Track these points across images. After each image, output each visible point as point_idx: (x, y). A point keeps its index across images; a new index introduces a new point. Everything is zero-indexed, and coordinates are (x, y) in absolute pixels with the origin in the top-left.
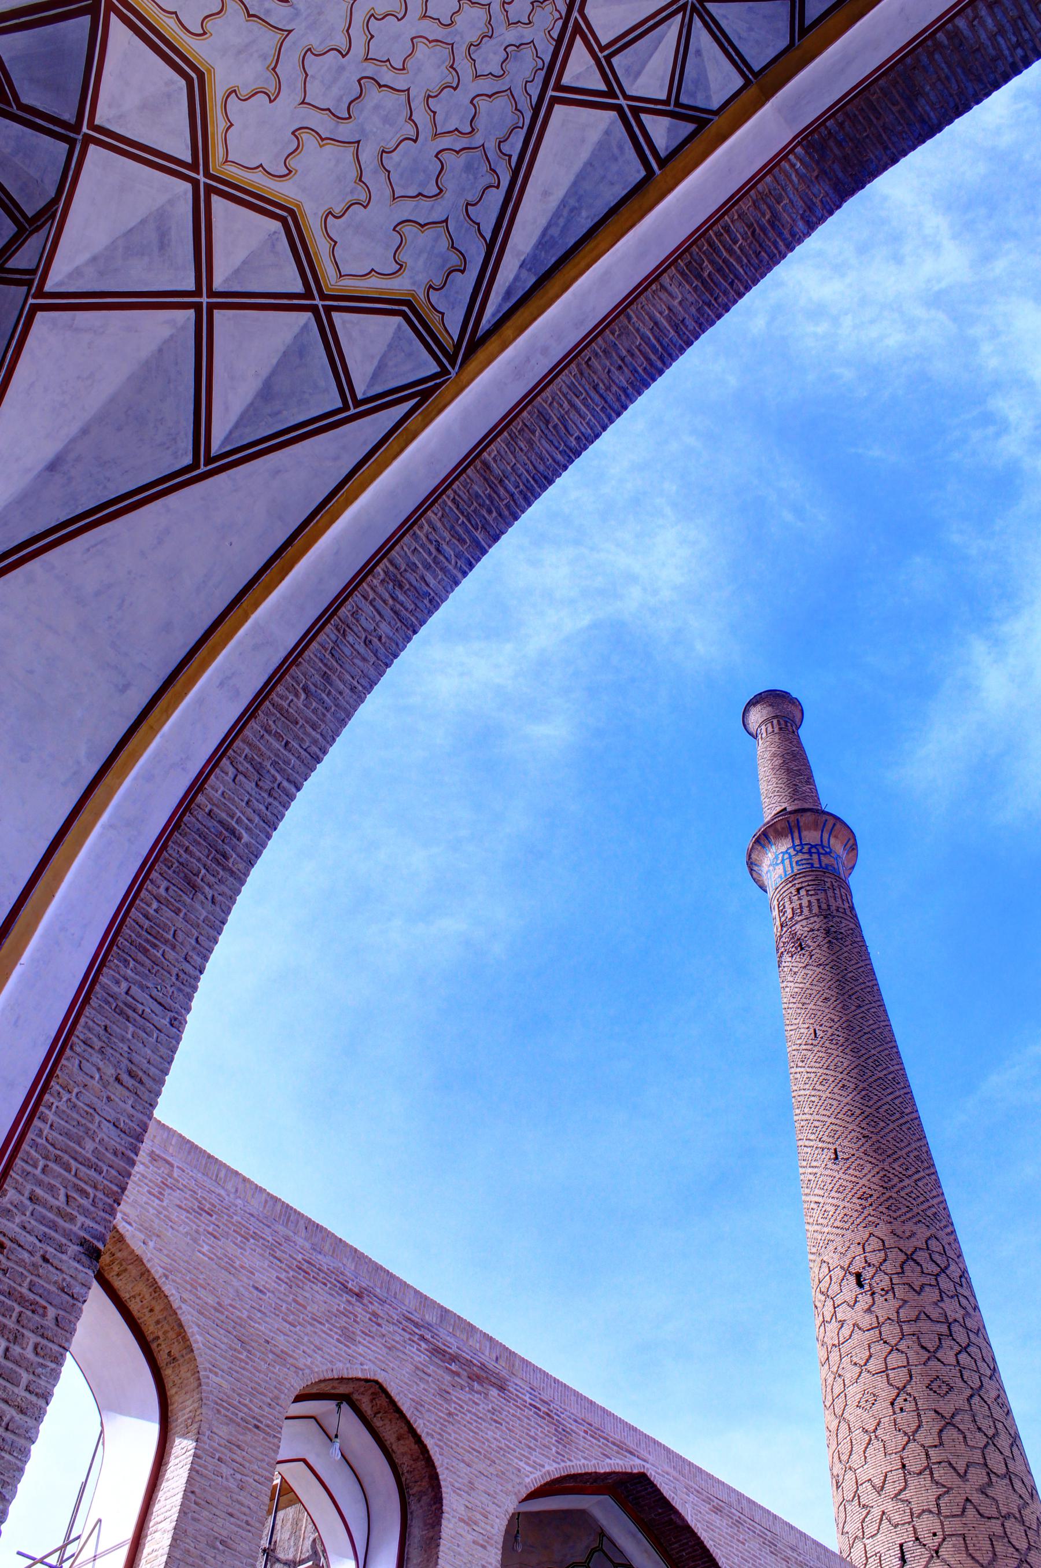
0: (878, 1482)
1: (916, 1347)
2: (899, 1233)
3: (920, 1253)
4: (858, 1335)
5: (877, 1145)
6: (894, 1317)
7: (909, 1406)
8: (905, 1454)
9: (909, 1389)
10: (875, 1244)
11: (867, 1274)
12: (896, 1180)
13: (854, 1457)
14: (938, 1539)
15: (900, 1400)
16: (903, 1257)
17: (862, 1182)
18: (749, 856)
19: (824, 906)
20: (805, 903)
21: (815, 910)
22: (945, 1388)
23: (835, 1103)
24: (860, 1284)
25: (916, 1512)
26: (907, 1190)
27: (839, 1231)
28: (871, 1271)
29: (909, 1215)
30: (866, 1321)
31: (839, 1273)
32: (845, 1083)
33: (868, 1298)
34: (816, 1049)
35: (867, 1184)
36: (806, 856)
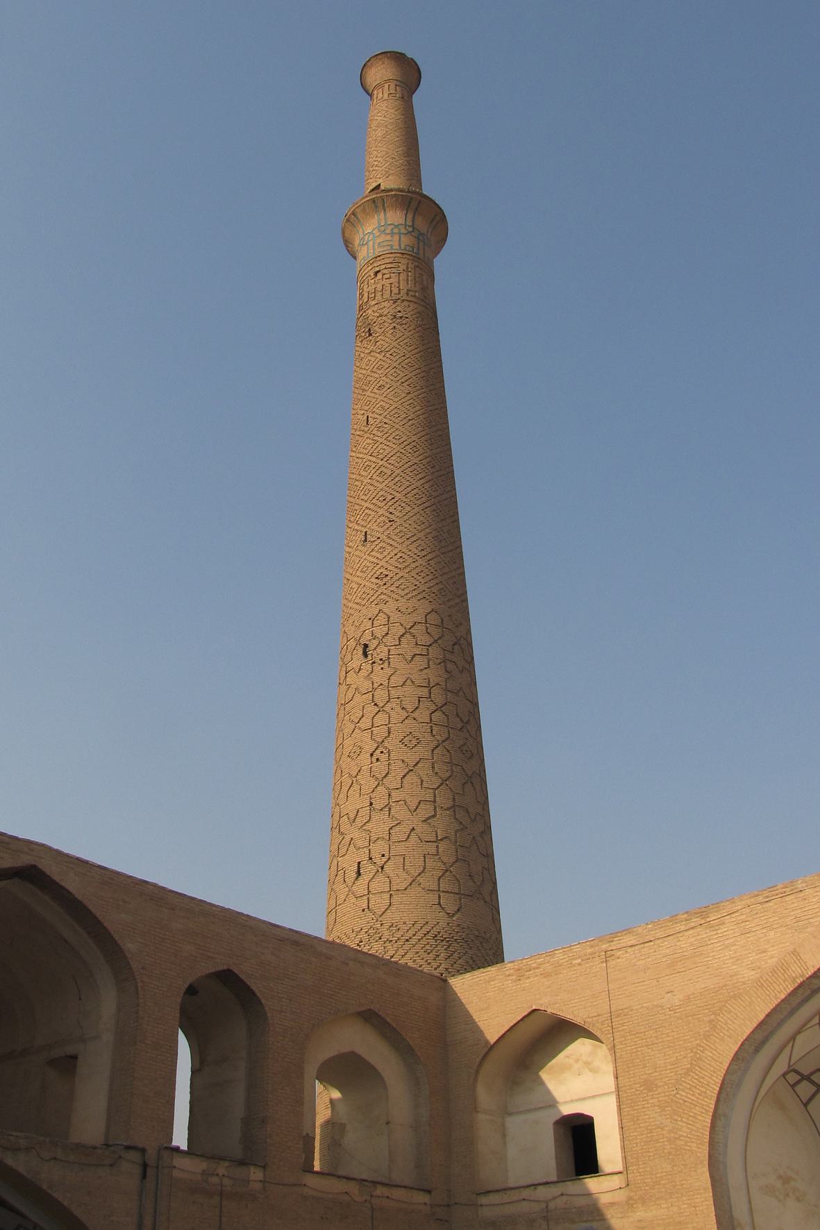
0: (352, 816)
1: (398, 709)
2: (403, 609)
3: (418, 627)
4: (358, 697)
5: (400, 528)
6: (386, 683)
7: (384, 757)
8: (373, 795)
9: (386, 744)
10: (382, 619)
11: (372, 645)
12: (411, 560)
13: (341, 796)
14: (384, 859)
15: (378, 752)
16: (402, 631)
17: (381, 563)
18: (343, 233)
19: (395, 290)
20: (379, 287)
21: (387, 295)
22: (414, 742)
23: (372, 488)
24: (365, 655)
25: (373, 838)
26: (417, 570)
27: (358, 607)
28: (375, 642)
29: (415, 593)
30: (366, 685)
31: (352, 643)
32: (383, 469)
33: (369, 667)
34: (366, 435)
35: (385, 565)
36: (389, 237)
